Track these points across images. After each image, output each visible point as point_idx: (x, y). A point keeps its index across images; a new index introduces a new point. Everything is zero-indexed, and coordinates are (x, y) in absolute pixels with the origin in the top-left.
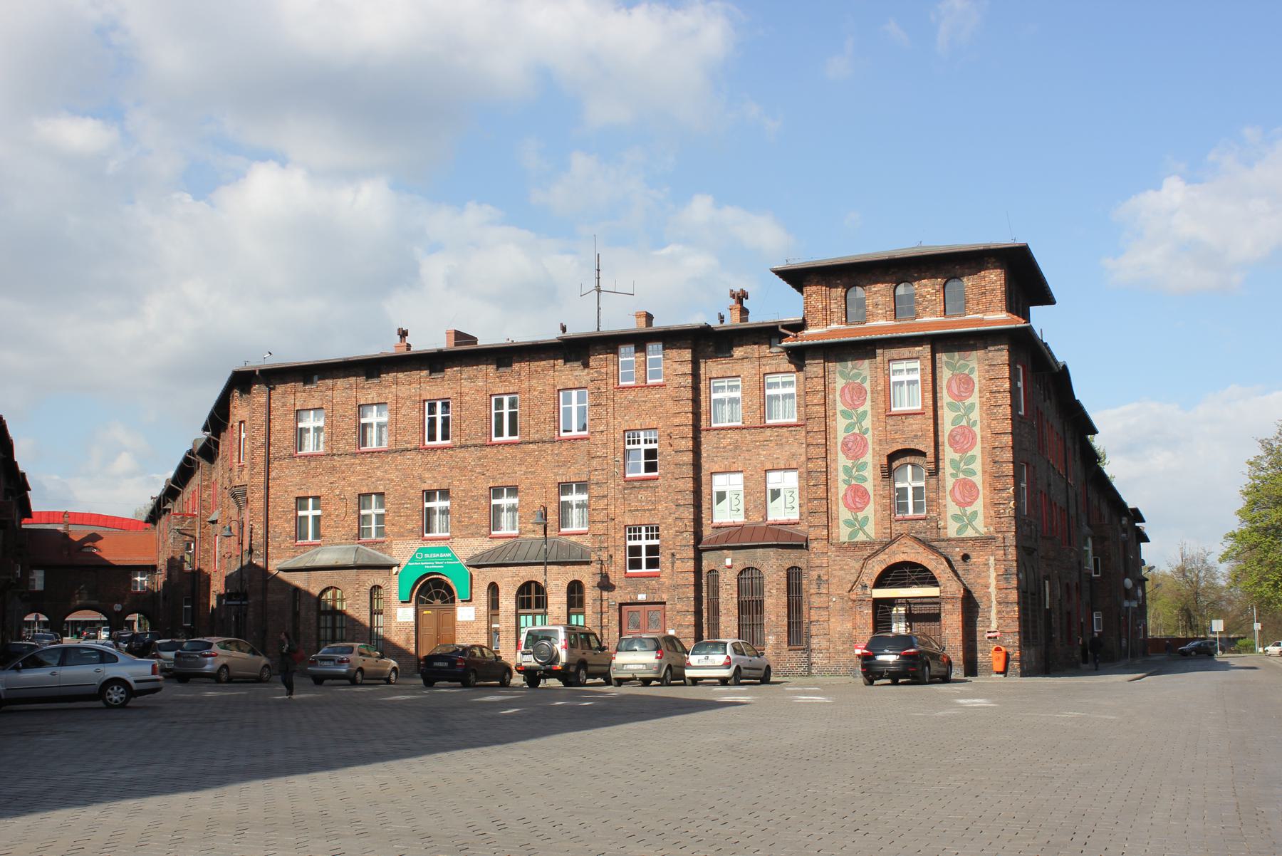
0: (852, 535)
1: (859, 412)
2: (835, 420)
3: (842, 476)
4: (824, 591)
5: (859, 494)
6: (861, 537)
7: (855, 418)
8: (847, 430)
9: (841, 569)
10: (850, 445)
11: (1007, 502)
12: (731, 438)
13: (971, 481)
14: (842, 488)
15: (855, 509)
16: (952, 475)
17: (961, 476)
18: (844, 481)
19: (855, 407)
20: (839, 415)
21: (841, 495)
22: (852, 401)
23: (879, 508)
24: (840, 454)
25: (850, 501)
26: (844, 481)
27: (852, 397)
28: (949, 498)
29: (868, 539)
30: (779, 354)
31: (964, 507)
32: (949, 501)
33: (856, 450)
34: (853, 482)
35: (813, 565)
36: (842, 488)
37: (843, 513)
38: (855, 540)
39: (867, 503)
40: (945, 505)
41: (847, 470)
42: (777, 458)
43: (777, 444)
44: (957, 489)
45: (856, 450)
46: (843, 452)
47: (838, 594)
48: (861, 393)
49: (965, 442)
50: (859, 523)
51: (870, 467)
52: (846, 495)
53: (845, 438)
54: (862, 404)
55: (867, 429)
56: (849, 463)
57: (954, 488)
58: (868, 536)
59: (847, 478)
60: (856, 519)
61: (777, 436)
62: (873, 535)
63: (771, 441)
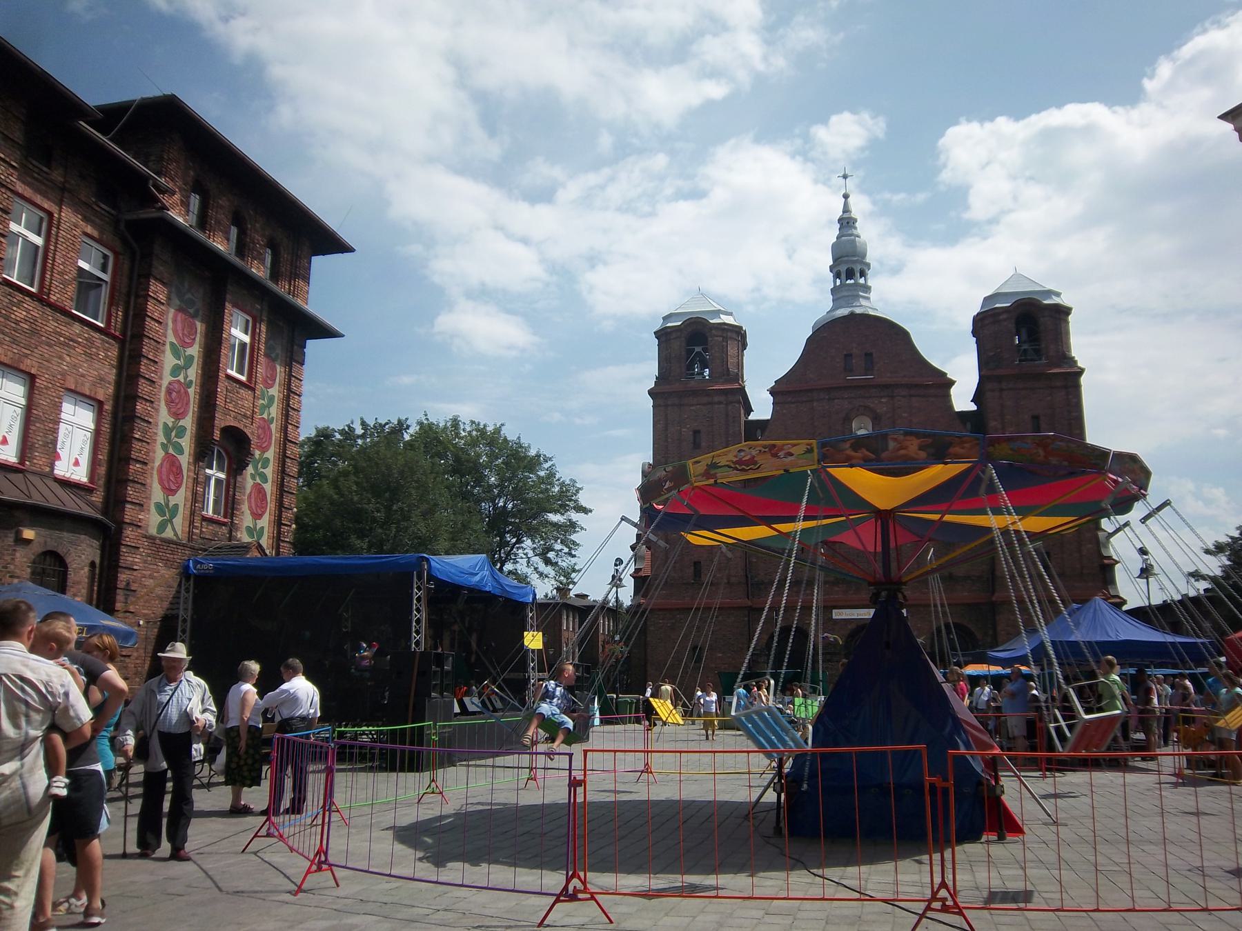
0: (162, 527)
1: (187, 354)
2: (163, 352)
3: (161, 438)
4: (132, 609)
5: (174, 469)
6: (168, 534)
7: (182, 360)
8: (176, 370)
9: (151, 577)
10: (174, 394)
11: (289, 524)
12: (28, 311)
13: (263, 488)
14: (159, 454)
15: (169, 491)
16: (253, 477)
17: (258, 481)
18: (162, 444)
19: (186, 345)
20: (168, 347)
21: (157, 463)
22: (183, 334)
23: (189, 494)
24: (163, 404)
25: (164, 477)
26: (162, 444)
27: (183, 330)
28: (246, 503)
29: (175, 538)
30: (107, 214)
31: (255, 520)
32: (245, 508)
33: (178, 407)
34: (171, 451)
35: (124, 565)
36: (159, 454)
37: (157, 494)
38: (164, 535)
39: (179, 487)
40: (243, 512)
41: (168, 430)
42: (83, 376)
43: (85, 353)
44: (253, 495)
45: (178, 407)
46: (167, 405)
47: (145, 615)
48: (192, 329)
49: (264, 440)
50: (169, 511)
51: (188, 433)
52: (161, 465)
53: (170, 384)
54: (191, 345)
55: (191, 382)
56: (170, 421)
57: (251, 493)
58: (176, 534)
59: (166, 442)
60: (167, 505)
61: (86, 339)
62: (179, 533)
63: (79, 343)
